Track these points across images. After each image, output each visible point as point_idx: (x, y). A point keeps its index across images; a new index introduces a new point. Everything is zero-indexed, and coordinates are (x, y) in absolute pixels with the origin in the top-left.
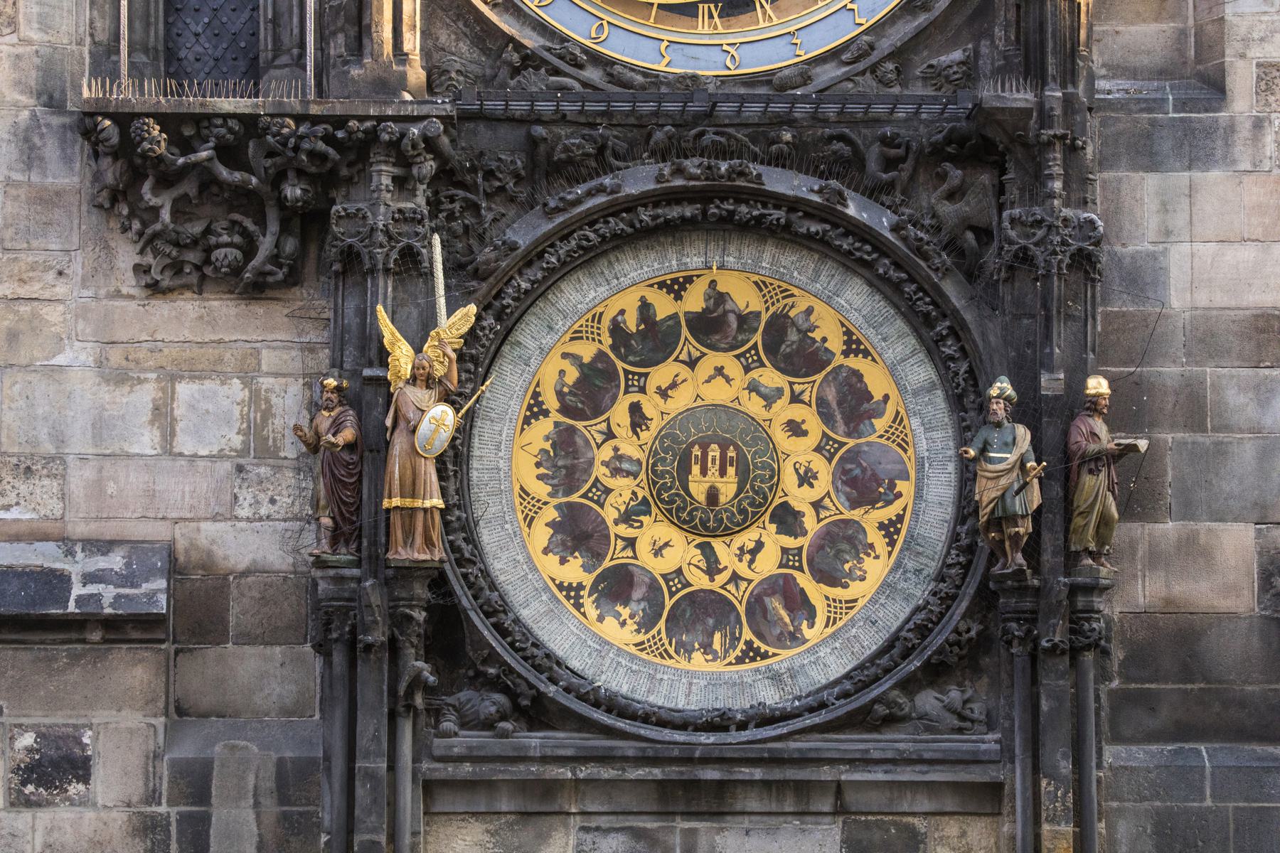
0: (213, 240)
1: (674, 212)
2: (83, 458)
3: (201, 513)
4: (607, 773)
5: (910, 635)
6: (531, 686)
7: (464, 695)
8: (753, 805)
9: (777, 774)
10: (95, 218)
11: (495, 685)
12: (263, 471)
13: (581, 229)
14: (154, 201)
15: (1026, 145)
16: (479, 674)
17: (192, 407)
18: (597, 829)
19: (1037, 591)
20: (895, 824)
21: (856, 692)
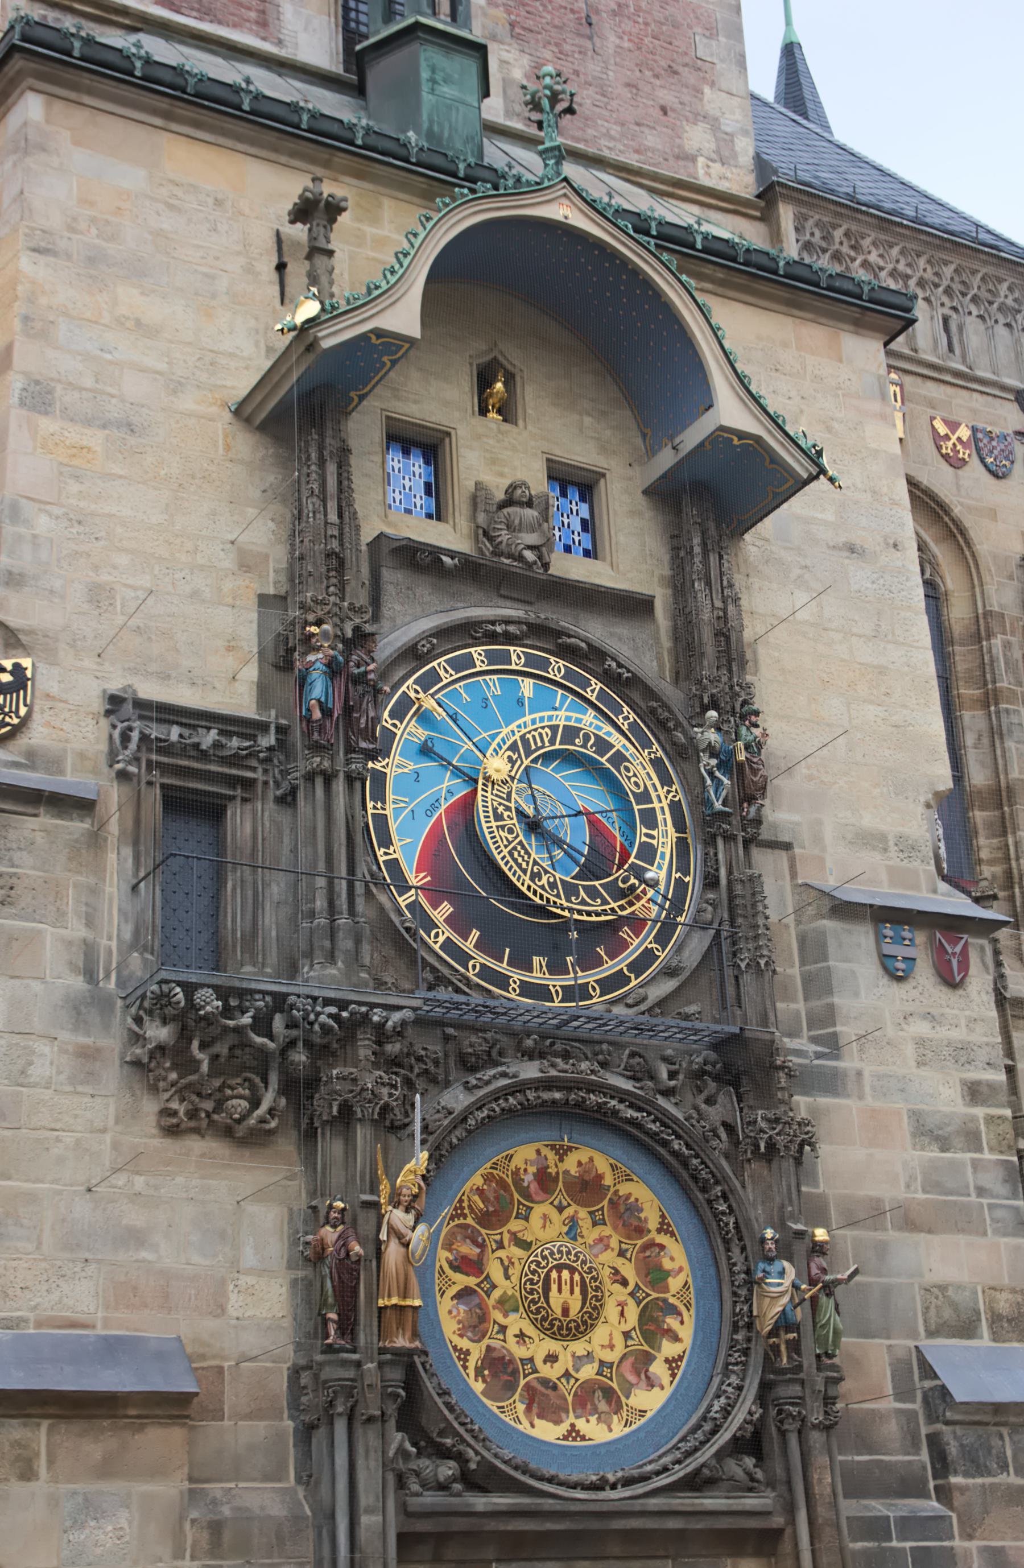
1: (546, 1096)
5: (717, 1415)
6: (477, 1453)
11: (444, 1454)
13: (490, 1102)
14: (200, 1056)
21: (686, 1458)
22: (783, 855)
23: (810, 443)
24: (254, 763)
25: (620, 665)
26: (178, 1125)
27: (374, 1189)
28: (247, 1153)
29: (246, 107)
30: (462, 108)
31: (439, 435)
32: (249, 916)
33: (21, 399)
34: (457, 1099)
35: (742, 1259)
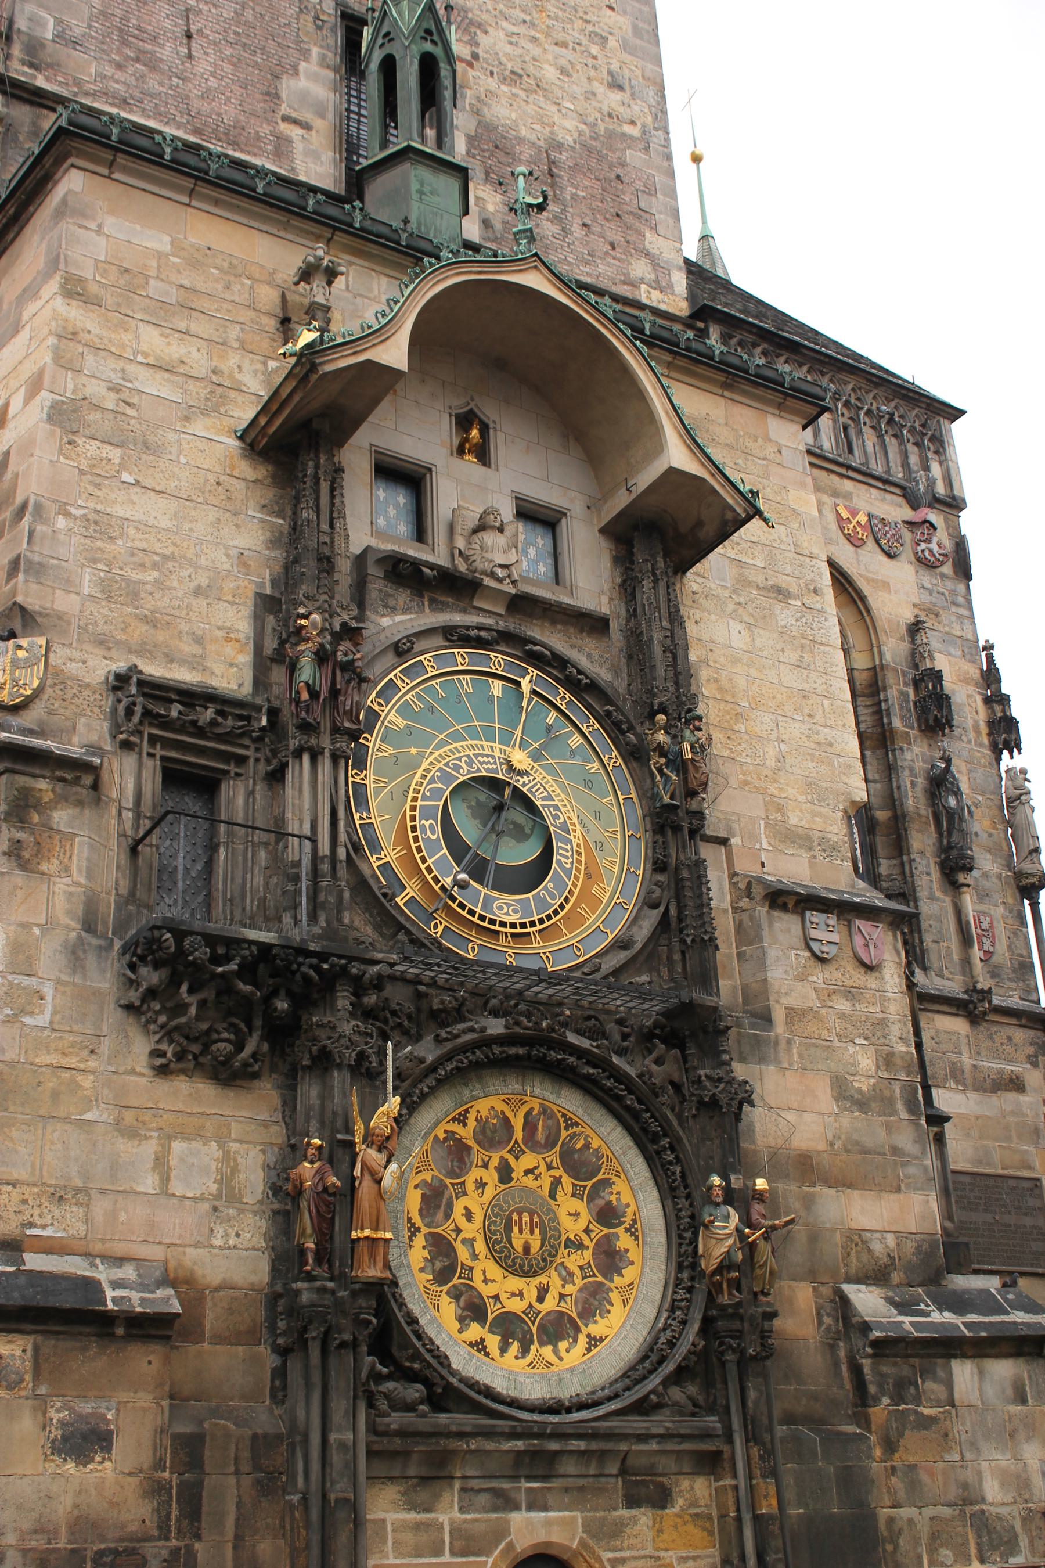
0: (215, 1036)
1: (512, 1051)
2: (102, 1192)
3: (187, 1241)
4: (490, 1445)
6: (443, 1378)
7: (391, 1385)
8: (571, 1469)
9: (594, 1446)
10: (120, 1013)
11: (412, 1377)
12: (231, 1211)
14: (189, 999)
15: (706, 1032)
16: (399, 1366)
17: (182, 1160)
18: (472, 1489)
19: (741, 1318)
20: (651, 1481)
21: (635, 1385)
22: (723, 848)
23: (747, 488)
24: (246, 741)
25: (580, 672)
26: (167, 1066)
27: (349, 1130)
28: (232, 1094)
29: (260, 190)
30: (445, 216)
31: (423, 471)
32: (239, 880)
33: (48, 415)
34: (428, 1051)
35: (687, 1204)
